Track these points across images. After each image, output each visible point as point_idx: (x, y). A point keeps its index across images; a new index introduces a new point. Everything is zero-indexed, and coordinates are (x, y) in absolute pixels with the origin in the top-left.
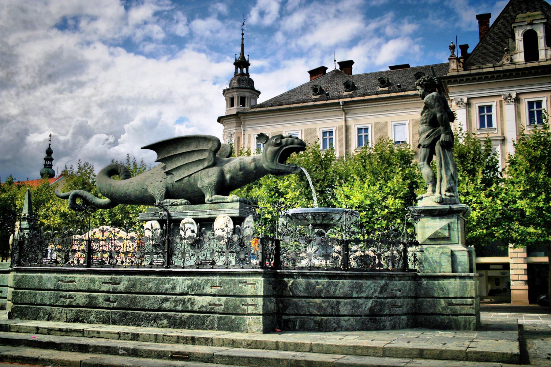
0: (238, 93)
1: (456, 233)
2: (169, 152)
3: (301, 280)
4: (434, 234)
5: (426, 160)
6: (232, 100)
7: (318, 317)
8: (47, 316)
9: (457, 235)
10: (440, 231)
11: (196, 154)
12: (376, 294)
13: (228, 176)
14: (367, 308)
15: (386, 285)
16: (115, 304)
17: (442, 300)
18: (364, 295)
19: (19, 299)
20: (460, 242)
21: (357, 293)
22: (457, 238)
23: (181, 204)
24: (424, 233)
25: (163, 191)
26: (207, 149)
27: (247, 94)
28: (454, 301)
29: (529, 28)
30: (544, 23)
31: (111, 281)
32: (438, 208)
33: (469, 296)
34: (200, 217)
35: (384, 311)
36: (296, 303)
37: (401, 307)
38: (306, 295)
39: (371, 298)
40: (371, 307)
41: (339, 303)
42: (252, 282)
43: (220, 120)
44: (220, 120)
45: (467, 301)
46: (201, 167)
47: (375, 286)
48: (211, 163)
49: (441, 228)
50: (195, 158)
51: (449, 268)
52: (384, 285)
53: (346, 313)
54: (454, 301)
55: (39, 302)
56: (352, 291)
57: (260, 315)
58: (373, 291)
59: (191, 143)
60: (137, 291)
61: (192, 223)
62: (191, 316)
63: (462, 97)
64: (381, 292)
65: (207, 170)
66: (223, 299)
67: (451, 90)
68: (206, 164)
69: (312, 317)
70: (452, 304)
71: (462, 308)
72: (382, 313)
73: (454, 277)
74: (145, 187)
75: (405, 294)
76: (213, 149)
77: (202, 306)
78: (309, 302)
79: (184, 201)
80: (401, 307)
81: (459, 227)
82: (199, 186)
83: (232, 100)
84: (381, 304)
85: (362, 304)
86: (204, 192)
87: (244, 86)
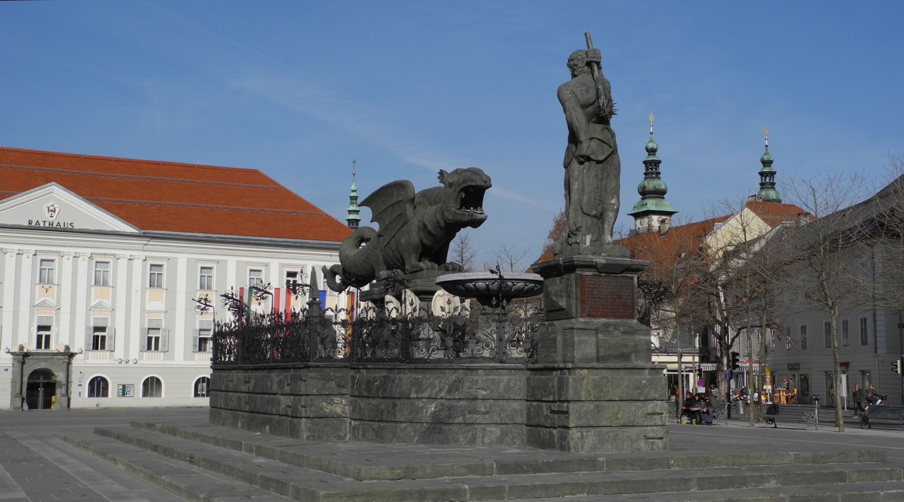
12: (443, 394)
14: (429, 413)
15: (459, 381)
17: (544, 404)
18: (426, 395)
21: (416, 392)
35: (454, 418)
37: (487, 413)
39: (435, 399)
40: (435, 412)
41: (394, 406)
47: (440, 382)
52: (455, 381)
53: (402, 419)
56: (410, 390)
58: (437, 389)
64: (449, 391)
66: (292, 397)
70: (553, 412)
72: (451, 421)
75: (495, 395)
80: (487, 413)
84: (450, 408)
85: (422, 408)
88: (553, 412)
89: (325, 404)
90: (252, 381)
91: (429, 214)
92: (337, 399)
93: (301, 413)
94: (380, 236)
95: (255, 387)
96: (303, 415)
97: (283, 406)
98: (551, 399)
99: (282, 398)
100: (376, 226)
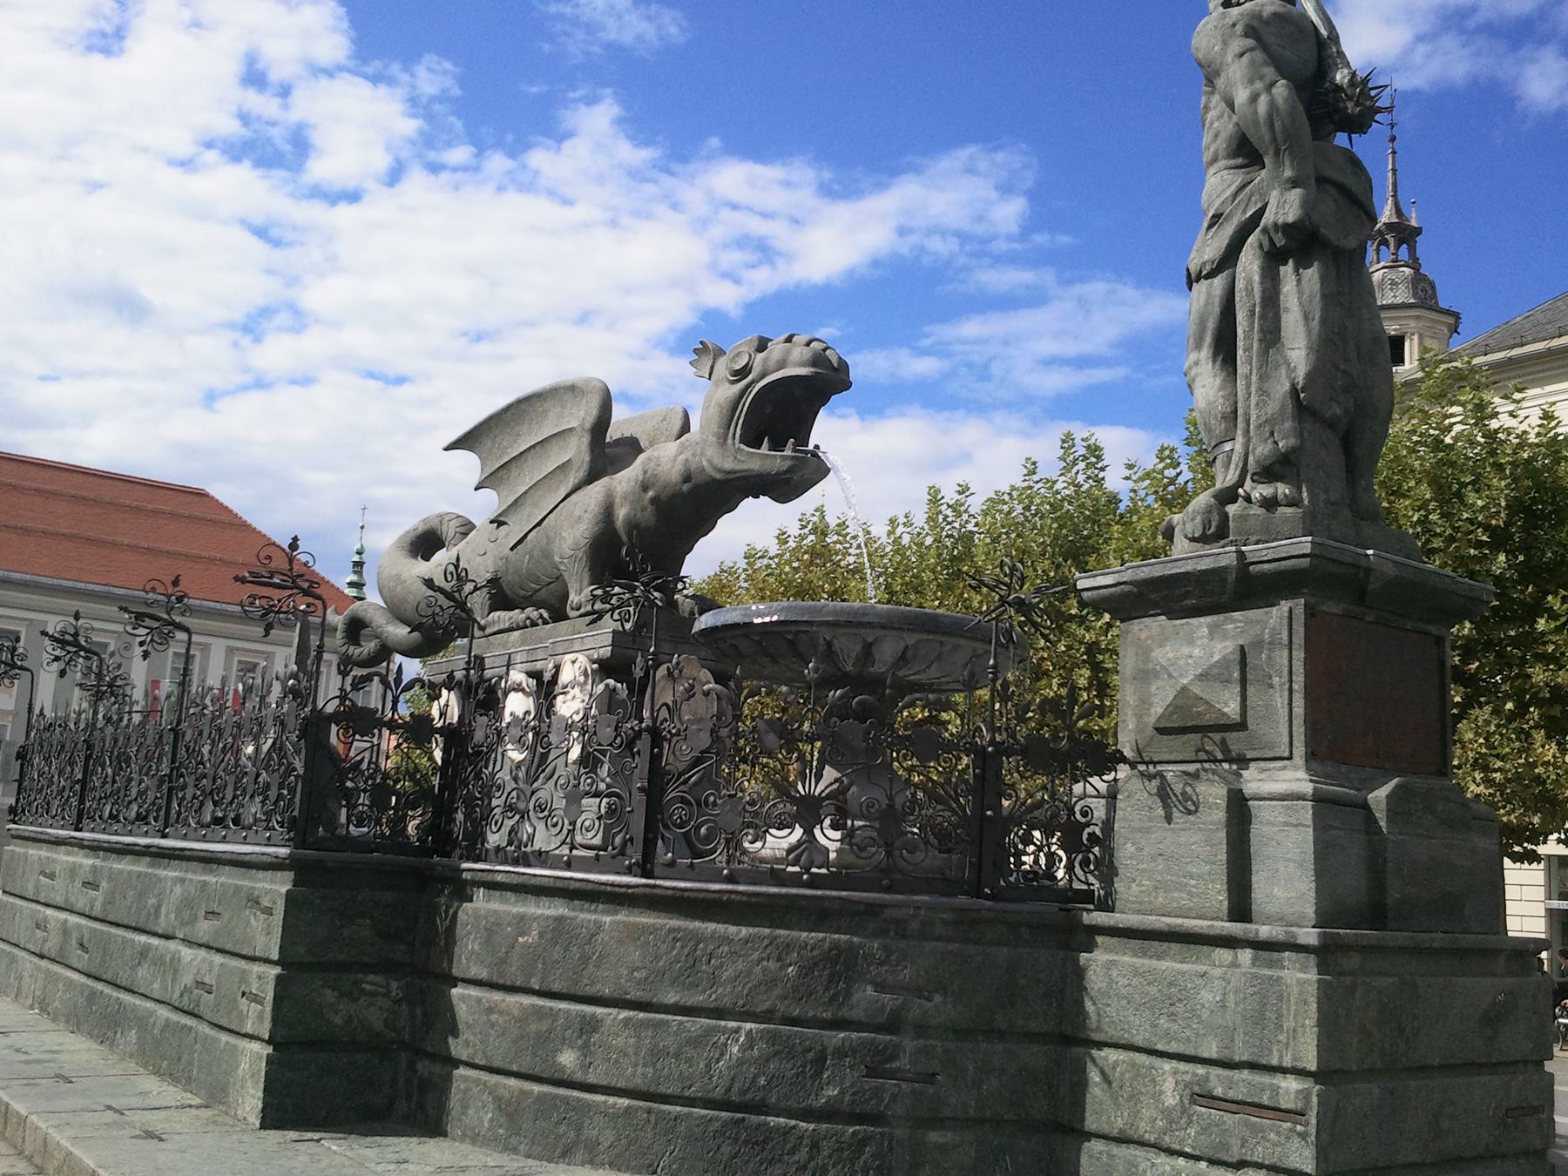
1: (1280, 701)
2: (504, 450)
4: (1175, 708)
5: (1208, 339)
7: (512, 1082)
9: (1281, 710)
10: (1196, 689)
13: (621, 513)
17: (1168, 1066)
20: (1299, 751)
22: (1285, 731)
24: (1145, 702)
26: (574, 424)
28: (1218, 1081)
32: (1204, 565)
33: (1287, 1062)
38: (483, 974)
40: (741, 1062)
42: (266, 903)
45: (1275, 1090)
48: (581, 474)
49: (1203, 677)
51: (1219, 896)
54: (1218, 1081)
65: (573, 497)
66: (218, 959)
69: (494, 1079)
70: (1205, 1097)
71: (1255, 1130)
73: (1230, 942)
76: (588, 424)
78: (490, 1010)
81: (1299, 667)
87: (1399, 300)
88: (1205, 1097)
89: (329, 995)
90: (104, 884)
91: (666, 459)
92: (372, 982)
93: (242, 1018)
94: (498, 522)
95: (109, 902)
96: (249, 1028)
97: (187, 979)
98: (1211, 1050)
99: (187, 953)
100: (487, 503)
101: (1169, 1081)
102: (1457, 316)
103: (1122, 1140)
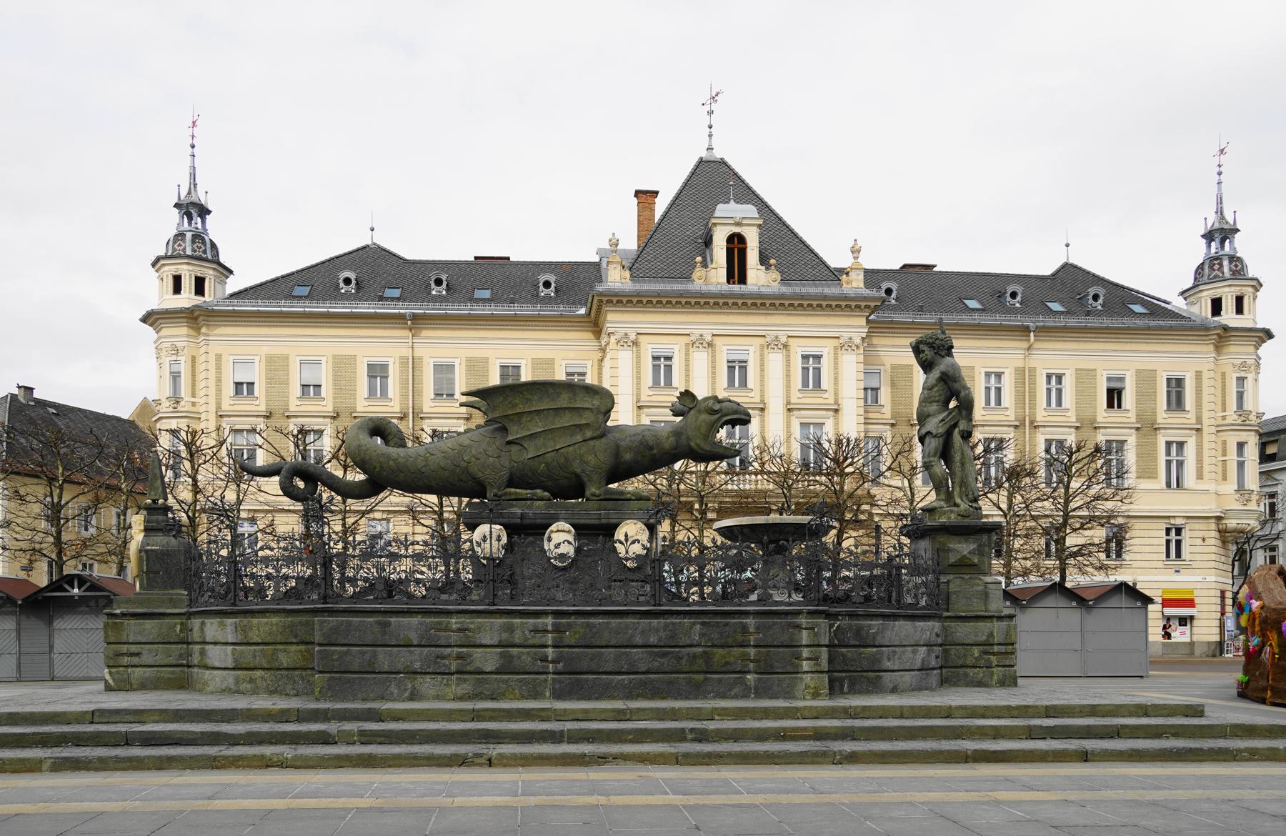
0: (190, 268)
2: (515, 406)
3: (846, 622)
6: (177, 281)
8: (407, 694)
11: (568, 415)
16: (560, 666)
19: (336, 664)
23: (542, 499)
25: (505, 474)
27: (209, 274)
29: (736, 230)
30: (759, 226)
31: (550, 628)
34: (582, 521)
36: (843, 655)
43: (150, 318)
44: (150, 318)
46: (579, 438)
50: (567, 420)
55: (386, 668)
57: (822, 672)
59: (559, 394)
60: (603, 643)
61: (569, 532)
62: (706, 679)
63: (628, 331)
65: (592, 443)
67: (610, 317)
68: (589, 434)
74: (463, 464)
77: (727, 663)
79: (546, 494)
82: (578, 471)
83: (177, 281)
86: (586, 479)
101: (976, 651)
102: (231, 272)
103: (962, 666)
